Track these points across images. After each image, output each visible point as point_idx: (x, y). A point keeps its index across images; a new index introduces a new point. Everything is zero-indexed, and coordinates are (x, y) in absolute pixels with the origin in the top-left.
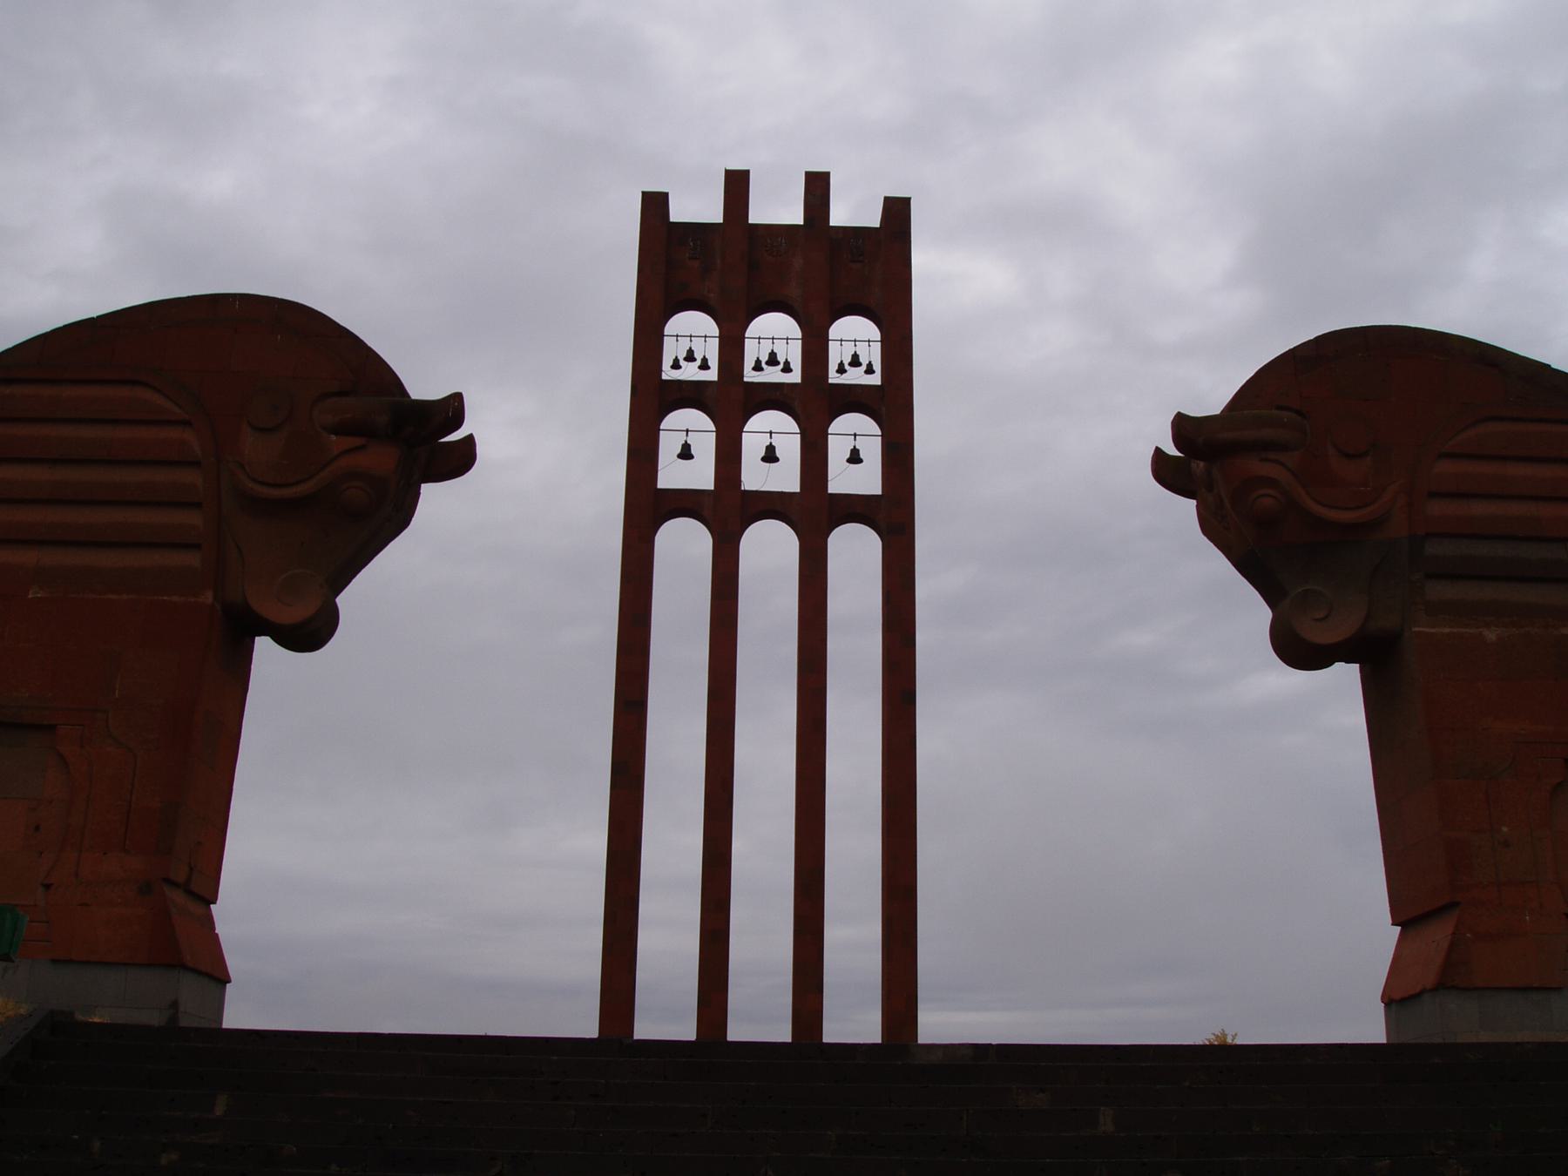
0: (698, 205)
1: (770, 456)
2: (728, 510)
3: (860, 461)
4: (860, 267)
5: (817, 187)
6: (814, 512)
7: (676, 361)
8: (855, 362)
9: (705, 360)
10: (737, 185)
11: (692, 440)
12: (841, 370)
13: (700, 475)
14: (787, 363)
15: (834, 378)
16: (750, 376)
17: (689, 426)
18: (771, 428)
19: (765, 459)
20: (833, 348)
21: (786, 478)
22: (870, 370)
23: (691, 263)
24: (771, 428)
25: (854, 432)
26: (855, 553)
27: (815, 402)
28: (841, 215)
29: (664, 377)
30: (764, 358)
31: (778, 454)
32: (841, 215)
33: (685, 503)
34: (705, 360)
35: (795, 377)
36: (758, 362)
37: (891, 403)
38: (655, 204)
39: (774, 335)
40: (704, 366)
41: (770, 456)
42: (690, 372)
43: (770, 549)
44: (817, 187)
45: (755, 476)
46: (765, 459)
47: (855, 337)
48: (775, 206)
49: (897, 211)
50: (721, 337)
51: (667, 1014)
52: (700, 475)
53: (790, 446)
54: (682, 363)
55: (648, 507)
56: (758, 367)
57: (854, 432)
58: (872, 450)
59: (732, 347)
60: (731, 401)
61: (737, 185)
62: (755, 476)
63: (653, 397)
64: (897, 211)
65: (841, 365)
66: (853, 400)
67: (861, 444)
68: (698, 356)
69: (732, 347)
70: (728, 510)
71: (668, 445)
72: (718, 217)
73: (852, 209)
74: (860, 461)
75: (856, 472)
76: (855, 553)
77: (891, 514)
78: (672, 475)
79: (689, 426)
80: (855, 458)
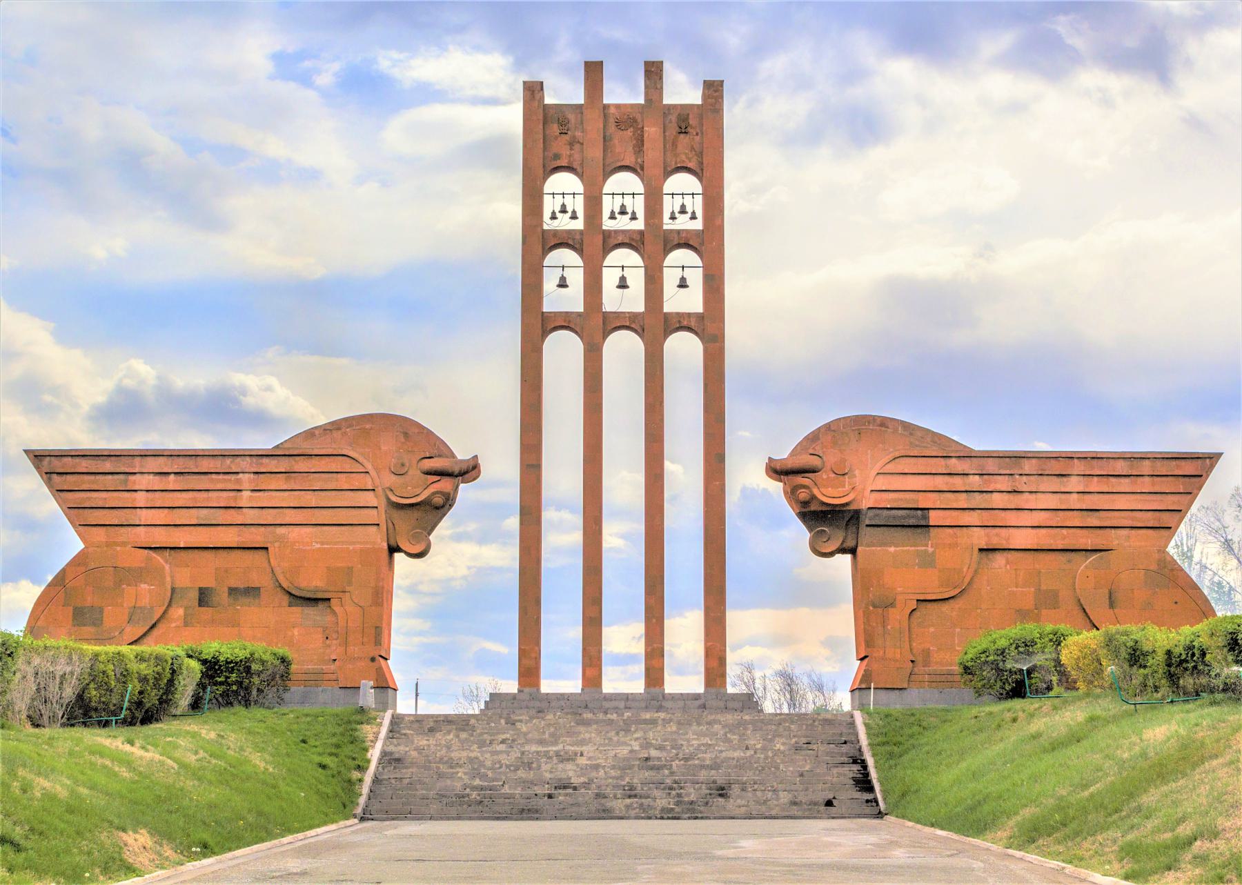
0: (565, 91)
1: (623, 285)
2: (594, 325)
3: (686, 286)
6: (655, 326)
7: (554, 213)
9: (574, 212)
11: (567, 273)
12: (673, 218)
13: (571, 300)
14: (634, 213)
15: (668, 225)
16: (608, 225)
18: (624, 261)
19: (619, 287)
21: (634, 301)
22: (693, 217)
24: (624, 261)
26: (684, 350)
27: (653, 243)
29: (545, 227)
30: (617, 210)
31: (629, 283)
34: (574, 212)
35: (639, 225)
36: (613, 212)
37: (707, 243)
39: (624, 188)
40: (574, 217)
41: (623, 285)
42: (564, 223)
43: (623, 350)
45: (612, 300)
46: (619, 287)
47: (682, 188)
48: (622, 92)
49: (714, 90)
50: (585, 194)
51: (559, 678)
52: (571, 300)
54: (558, 215)
55: (538, 325)
56: (612, 217)
58: (696, 278)
59: (593, 202)
60: (594, 244)
62: (612, 300)
63: (539, 241)
64: (714, 90)
65: (673, 213)
66: (684, 241)
67: (688, 273)
68: (569, 209)
69: (593, 202)
70: (594, 325)
72: (580, 99)
73: (682, 91)
74: (686, 286)
75: (685, 300)
76: (684, 350)
77: (708, 326)
80: (683, 284)
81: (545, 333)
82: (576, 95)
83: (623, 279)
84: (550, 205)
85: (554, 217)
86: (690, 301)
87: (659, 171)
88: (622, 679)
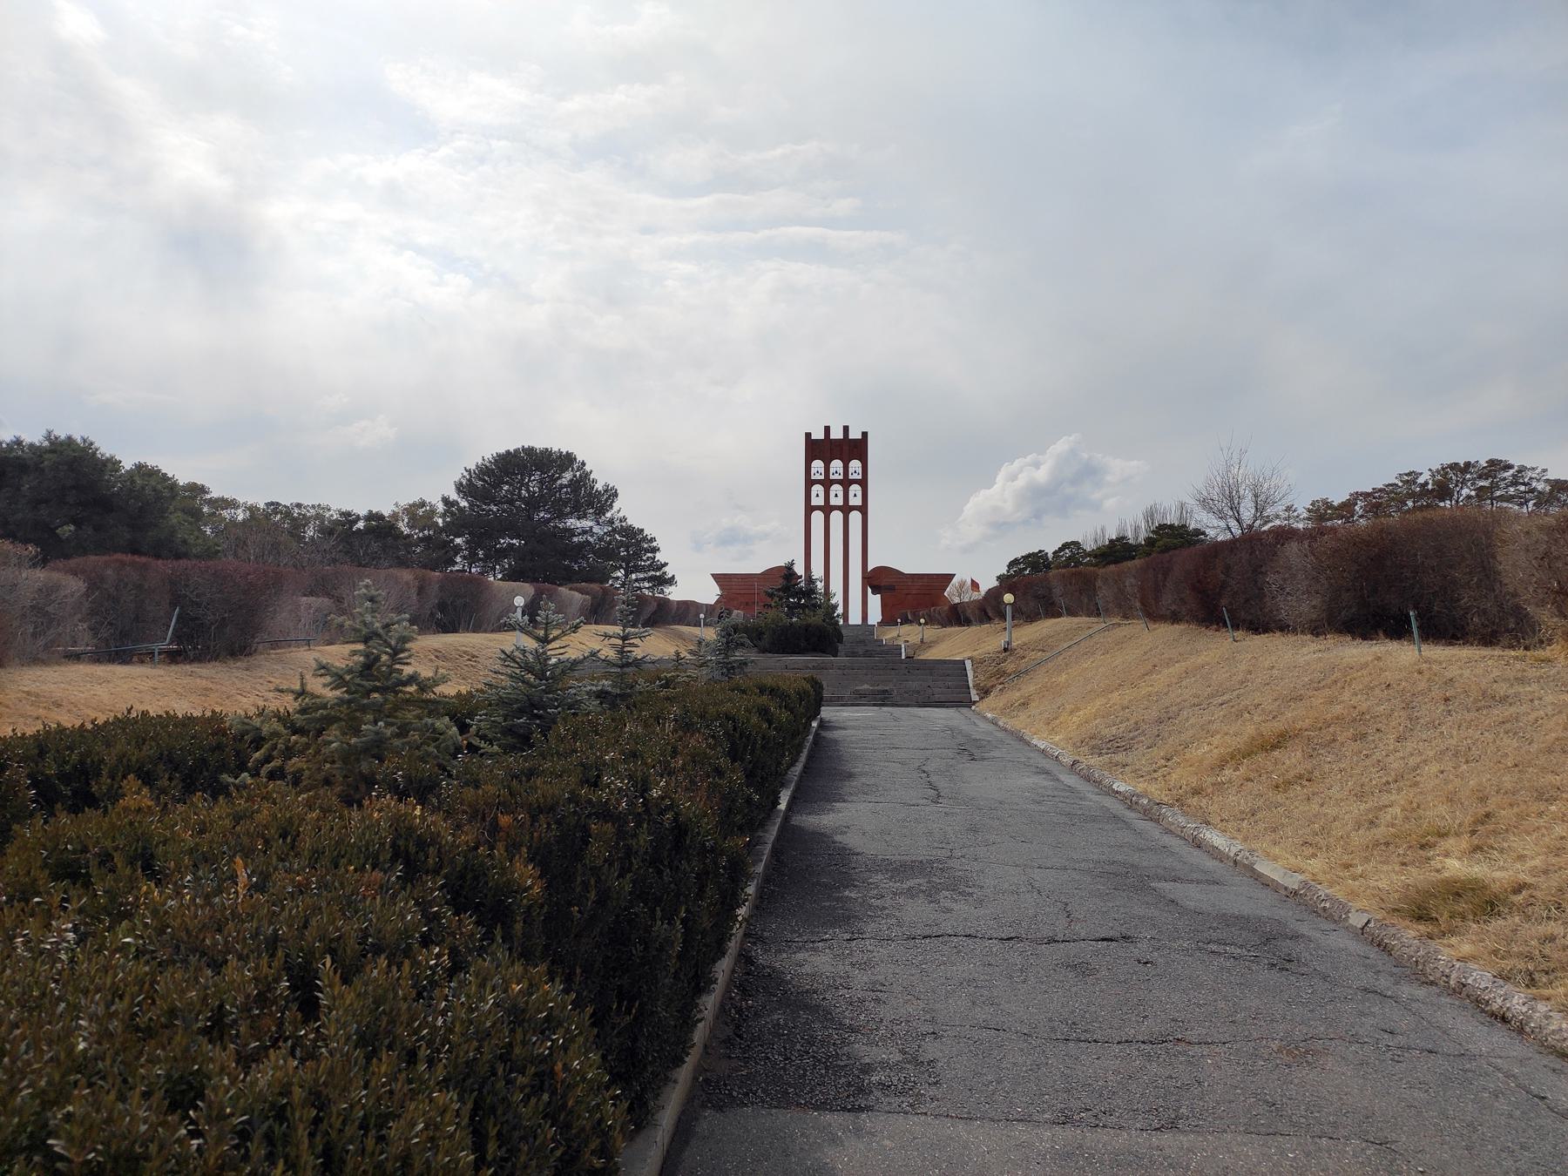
0: (818, 435)
2: (827, 509)
4: (854, 448)
5: (846, 429)
6: (846, 509)
10: (827, 429)
17: (818, 489)
18: (837, 489)
21: (839, 501)
23: (818, 449)
24: (837, 489)
25: (855, 489)
26: (855, 517)
27: (846, 483)
28: (852, 436)
32: (852, 436)
33: (818, 508)
37: (863, 483)
38: (808, 435)
39: (837, 465)
43: (836, 517)
44: (846, 429)
47: (855, 465)
48: (837, 434)
49: (865, 434)
53: (841, 494)
55: (809, 509)
57: (855, 489)
58: (859, 494)
60: (827, 483)
61: (827, 429)
62: (834, 501)
63: (810, 483)
64: (865, 434)
70: (827, 509)
73: (855, 434)
75: (855, 501)
76: (855, 517)
78: (816, 501)
79: (818, 489)
82: (822, 437)
84: (813, 471)
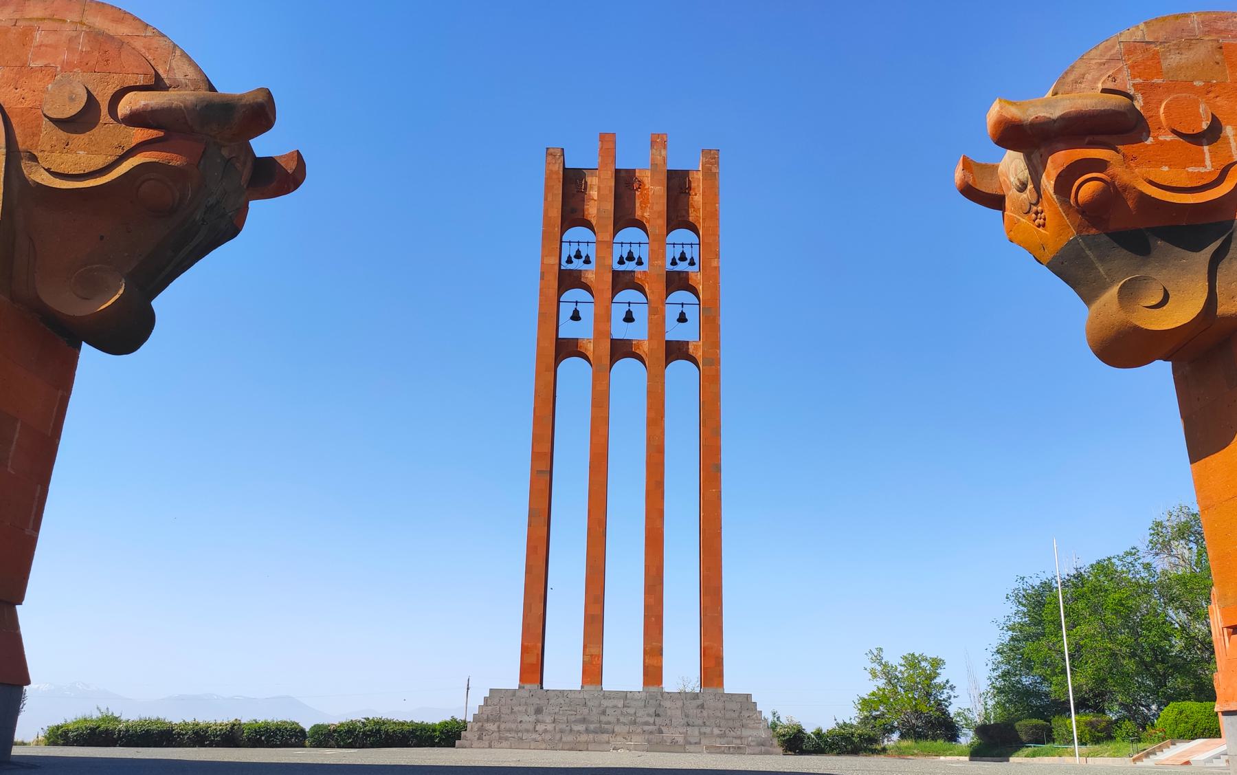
7: (569, 257)
8: (683, 258)
9: (587, 256)
20: (669, 248)
30: (625, 256)
34: (587, 256)
36: (621, 257)
51: (563, 670)
58: (692, 313)
67: (686, 309)
71: (566, 311)
78: (568, 330)
81: (558, 359)
83: (629, 313)
85: (569, 261)
86: (688, 333)
87: (662, 222)
88: (623, 671)
